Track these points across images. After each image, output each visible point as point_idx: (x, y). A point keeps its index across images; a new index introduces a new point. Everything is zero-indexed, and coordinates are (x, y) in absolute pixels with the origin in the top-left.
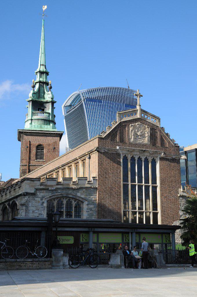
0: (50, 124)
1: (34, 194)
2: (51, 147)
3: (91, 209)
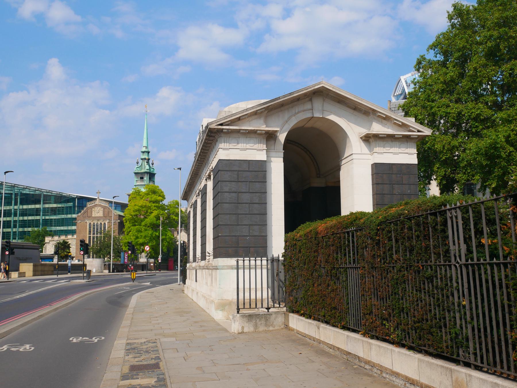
1: (49, 243)
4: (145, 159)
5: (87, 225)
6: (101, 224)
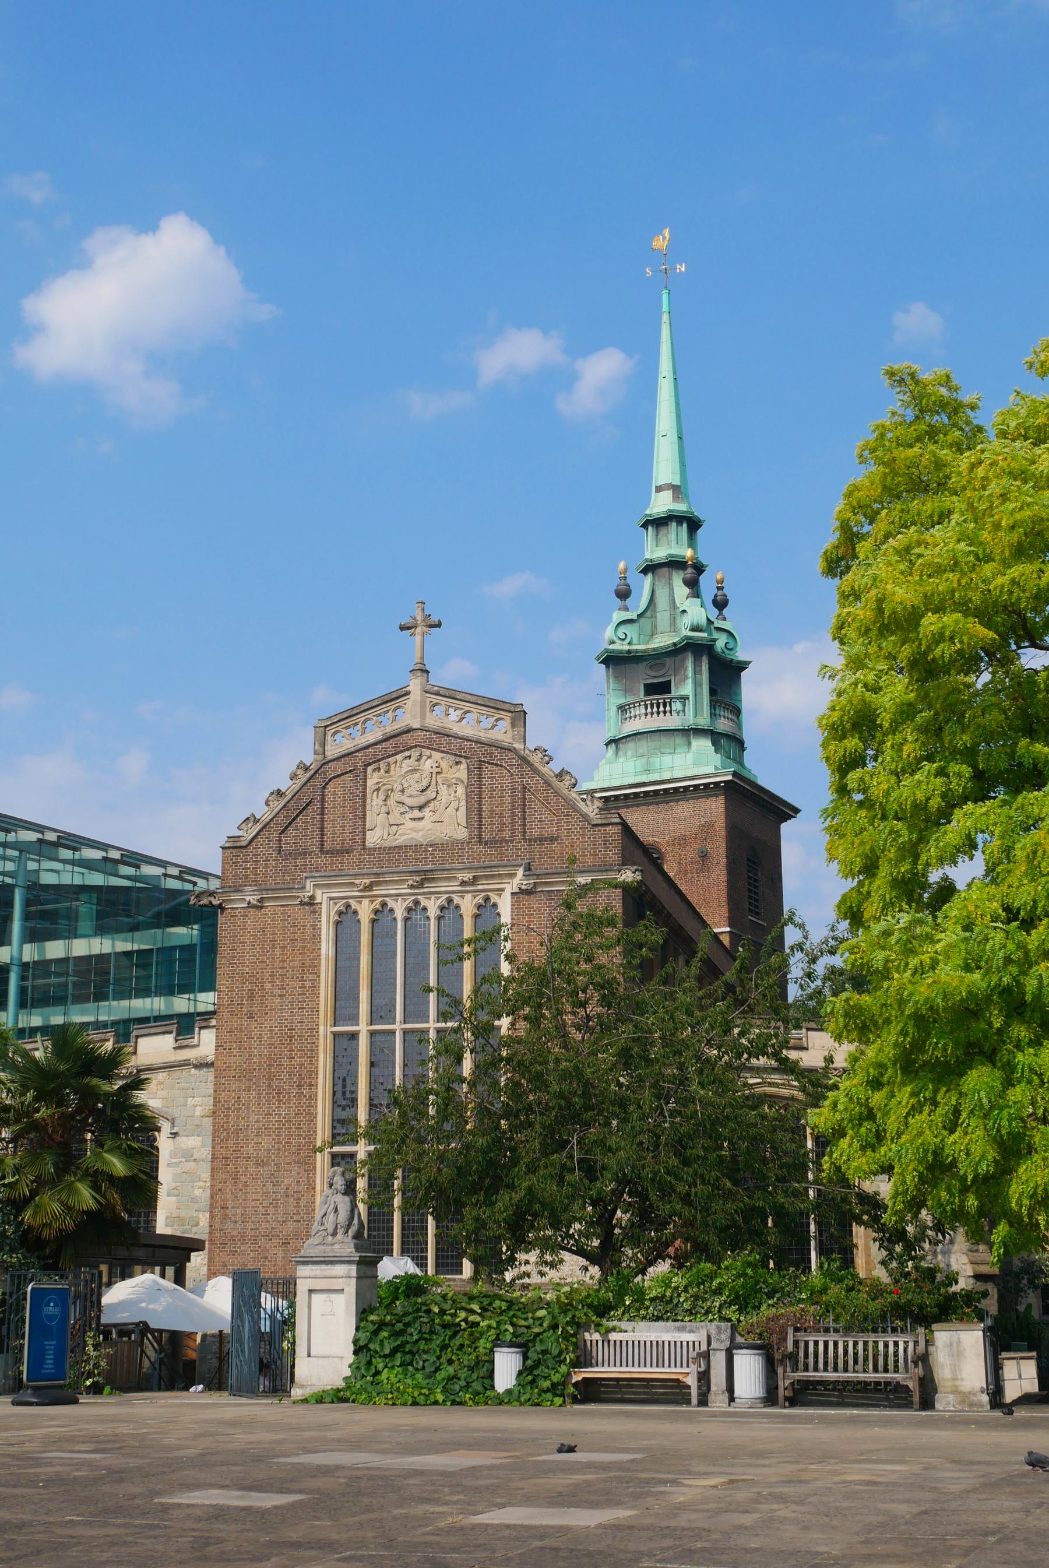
0: (689, 744)
2: (691, 853)
3: (188, 1155)
4: (675, 564)
5: (316, 928)
6: (449, 907)
